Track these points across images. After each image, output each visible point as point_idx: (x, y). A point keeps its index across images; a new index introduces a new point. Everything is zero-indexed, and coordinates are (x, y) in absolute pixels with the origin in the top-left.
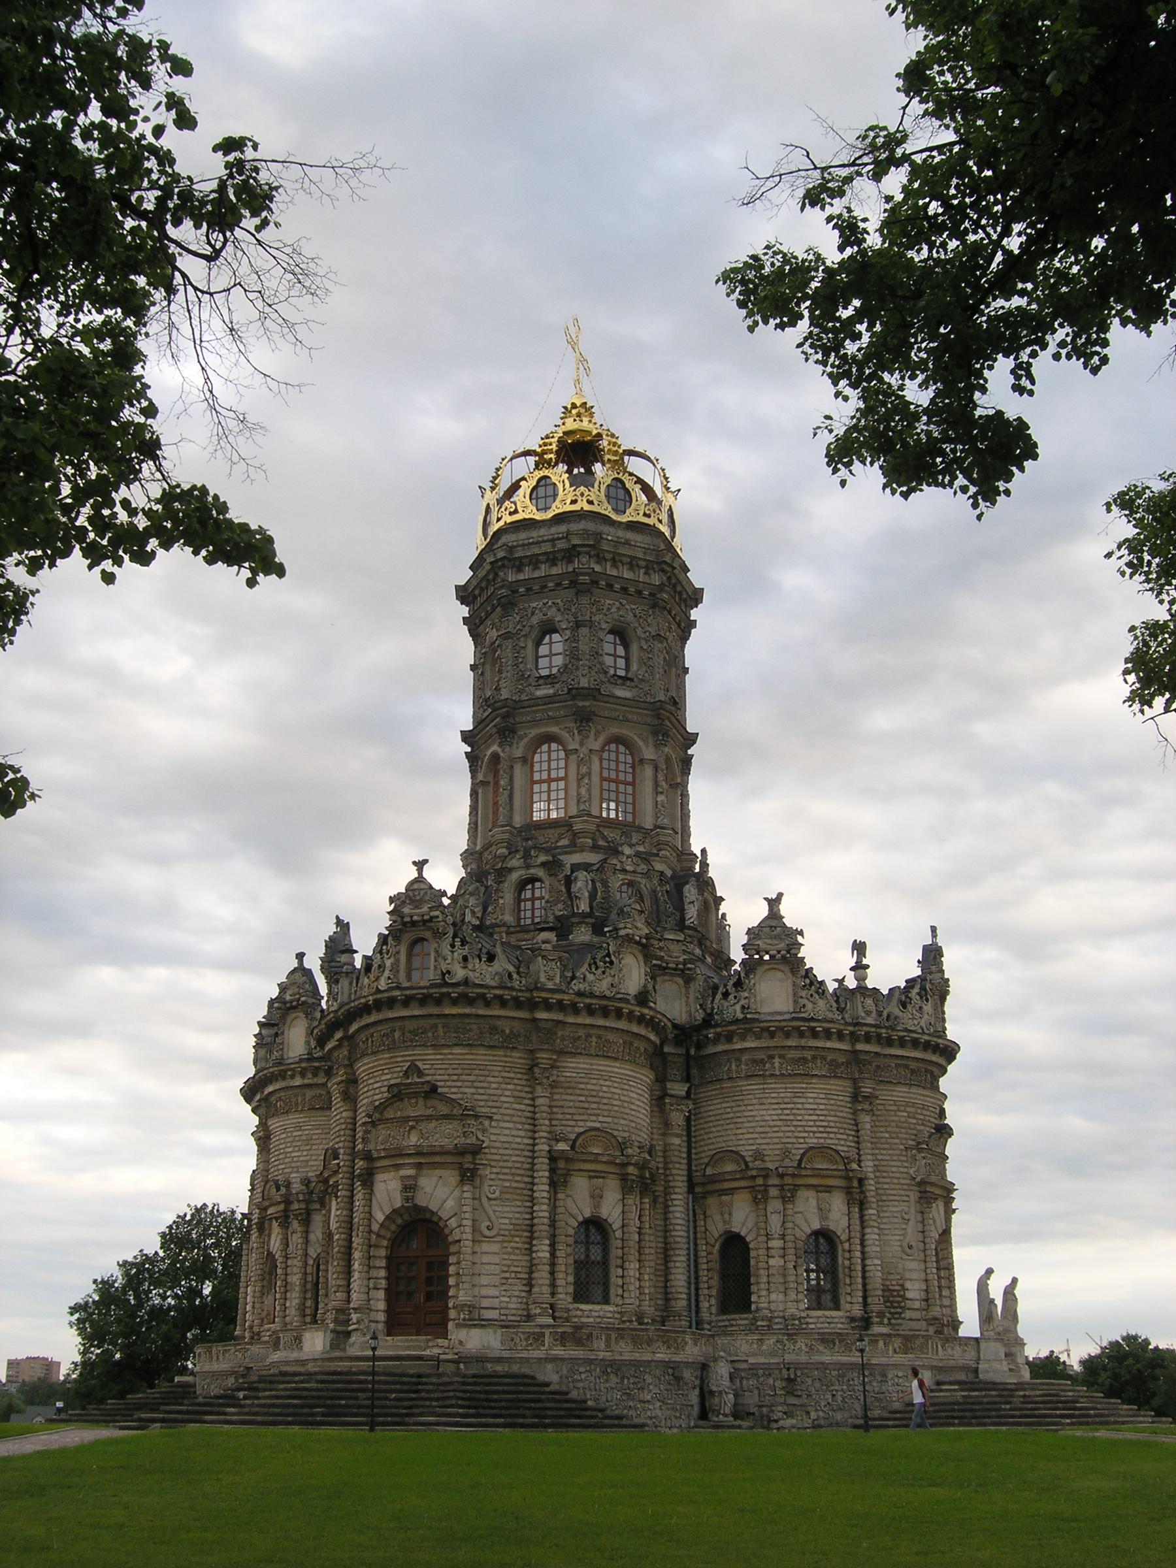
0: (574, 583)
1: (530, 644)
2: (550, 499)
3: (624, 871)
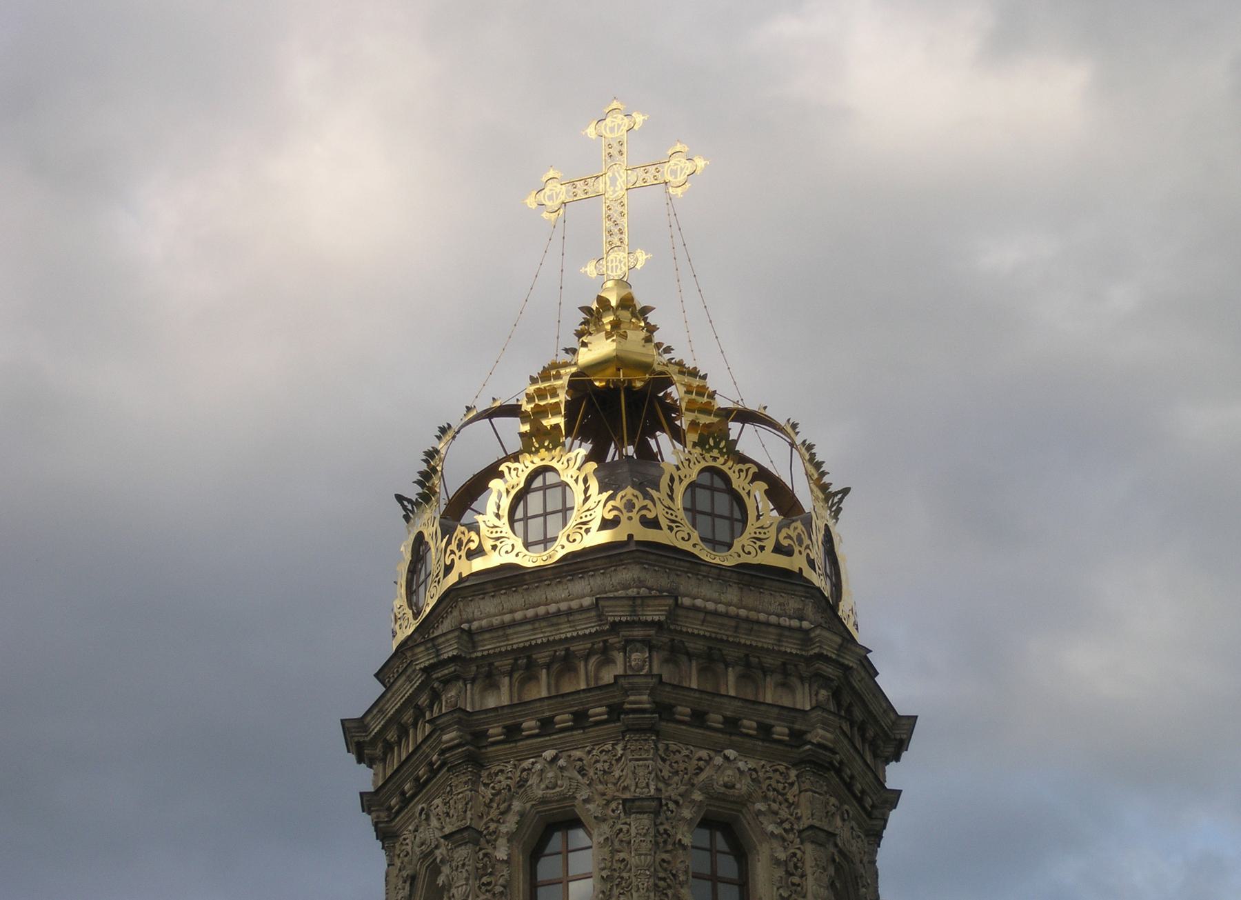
0: (615, 712)
1: (519, 859)
2: (554, 520)
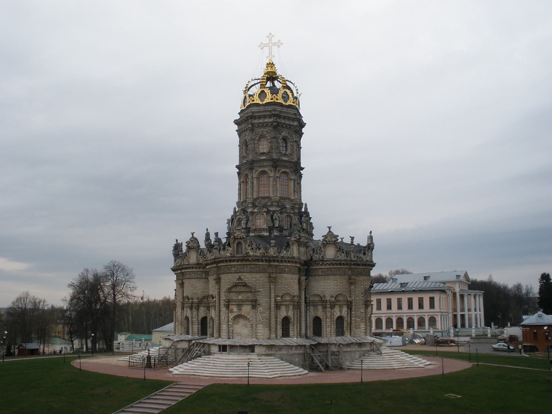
3: (287, 213)
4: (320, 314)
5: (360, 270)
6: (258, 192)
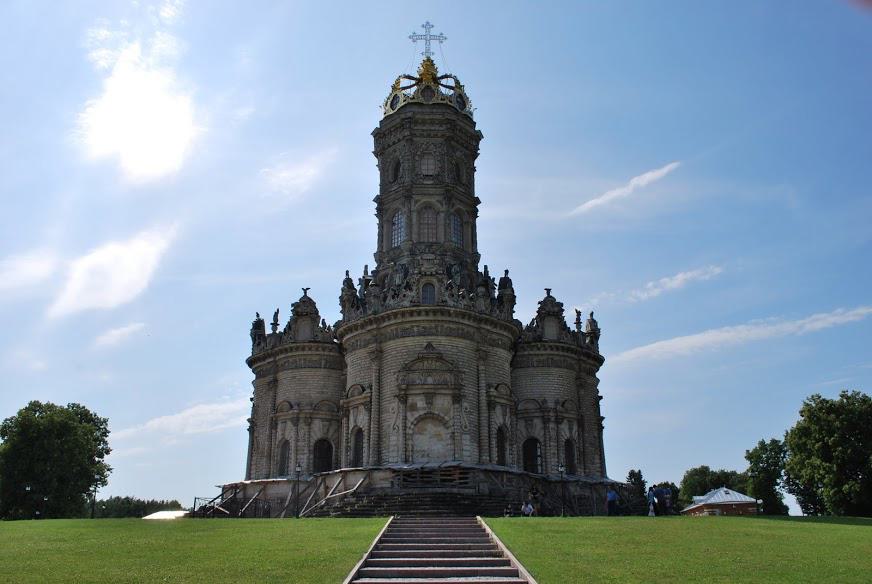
4: (538, 432)
5: (588, 366)
6: (419, 235)
